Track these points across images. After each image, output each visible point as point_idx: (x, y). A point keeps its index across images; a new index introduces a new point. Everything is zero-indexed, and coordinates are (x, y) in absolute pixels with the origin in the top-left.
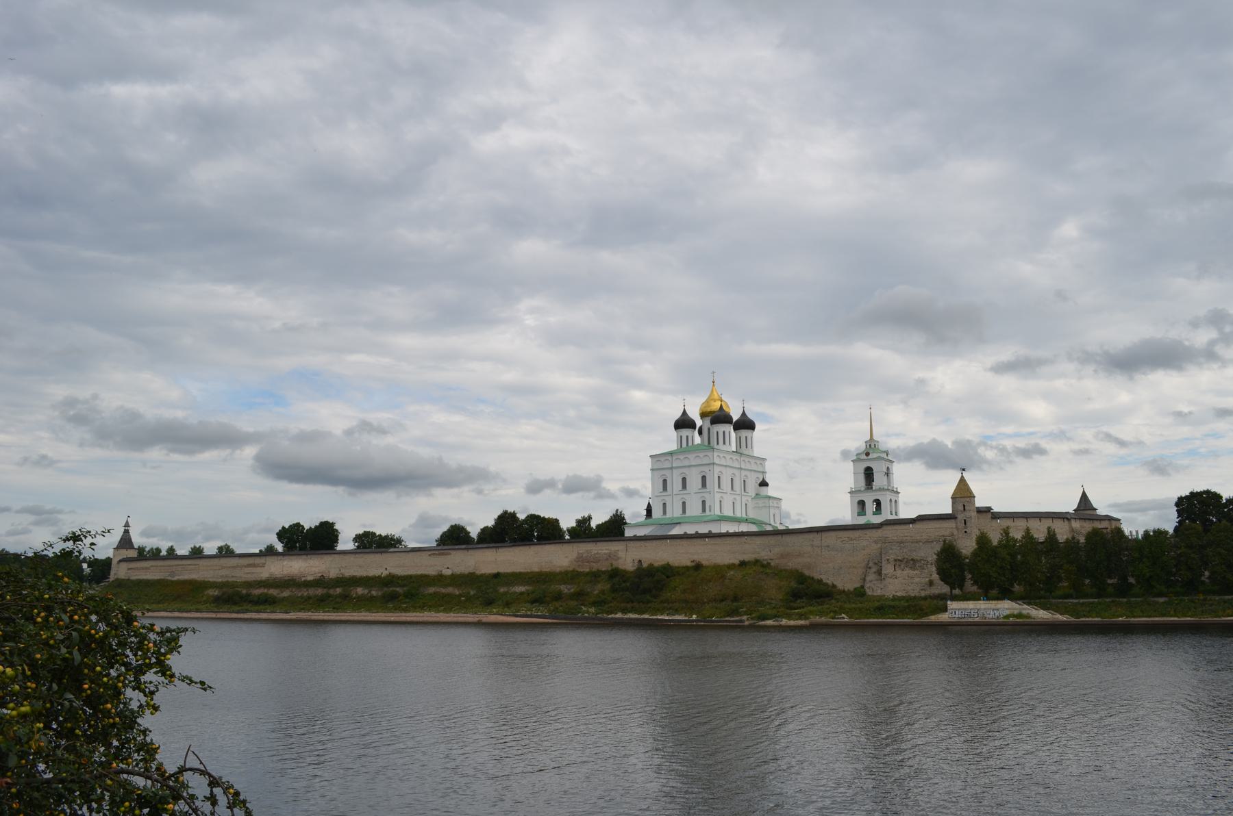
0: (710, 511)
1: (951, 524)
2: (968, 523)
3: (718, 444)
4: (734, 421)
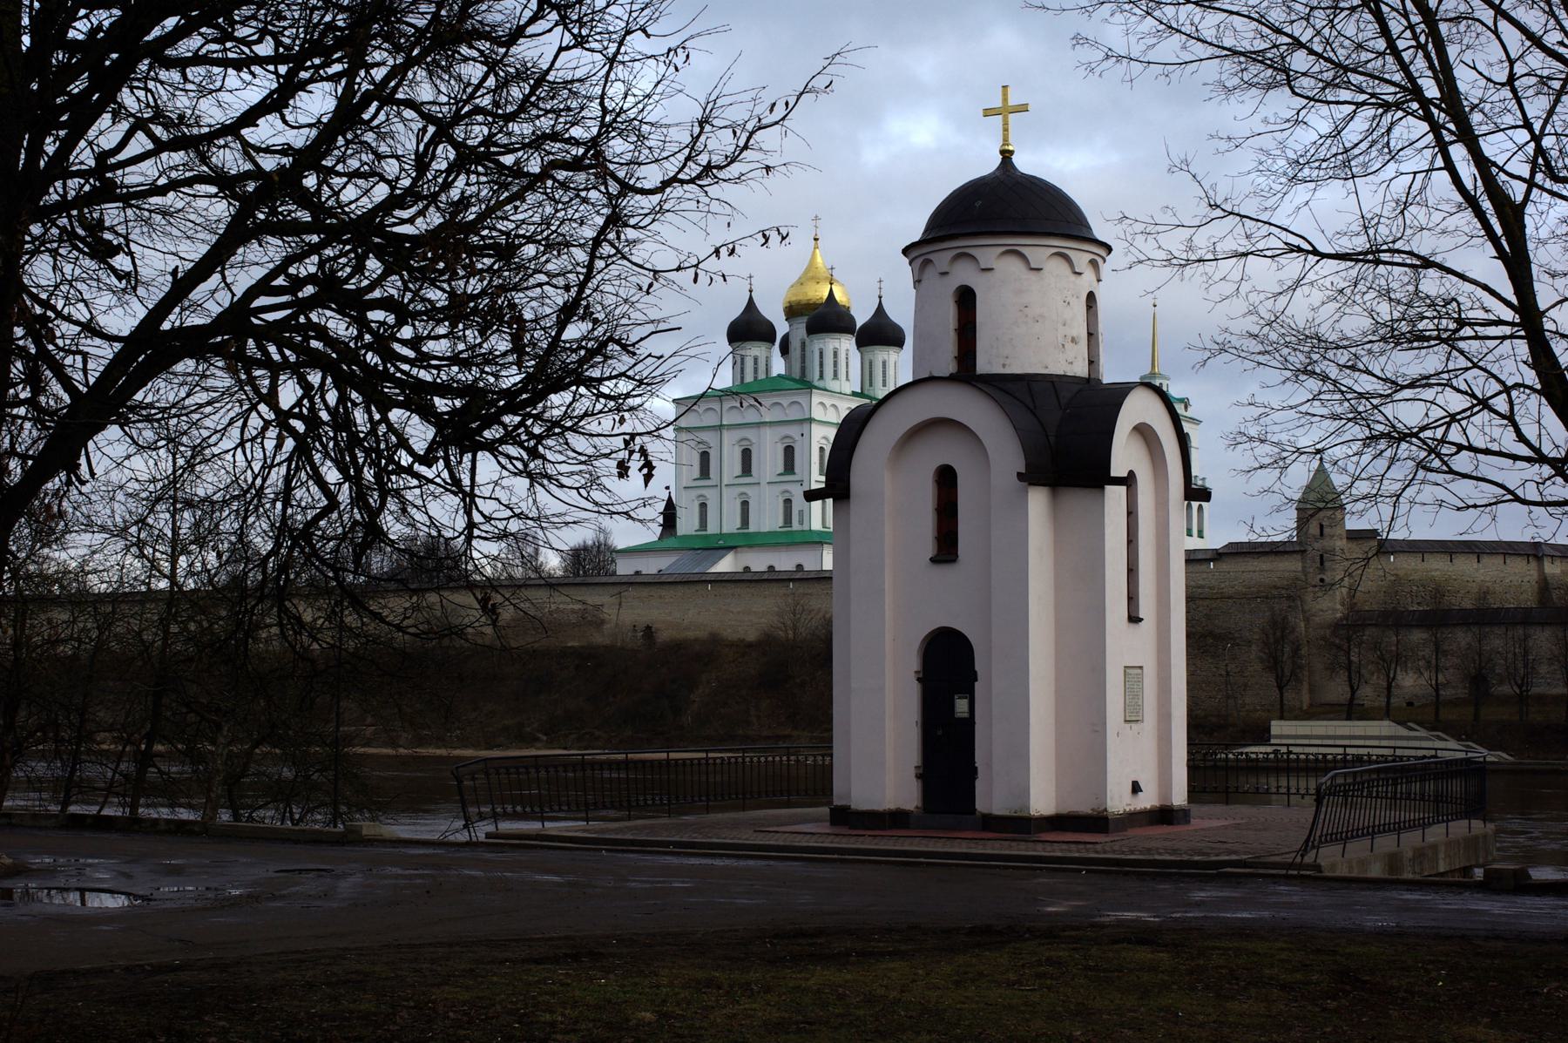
0: (801, 522)
1: (1291, 566)
2: (1327, 564)
3: (821, 377)
4: (859, 325)
